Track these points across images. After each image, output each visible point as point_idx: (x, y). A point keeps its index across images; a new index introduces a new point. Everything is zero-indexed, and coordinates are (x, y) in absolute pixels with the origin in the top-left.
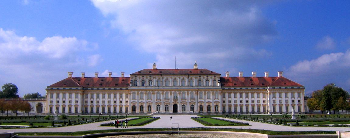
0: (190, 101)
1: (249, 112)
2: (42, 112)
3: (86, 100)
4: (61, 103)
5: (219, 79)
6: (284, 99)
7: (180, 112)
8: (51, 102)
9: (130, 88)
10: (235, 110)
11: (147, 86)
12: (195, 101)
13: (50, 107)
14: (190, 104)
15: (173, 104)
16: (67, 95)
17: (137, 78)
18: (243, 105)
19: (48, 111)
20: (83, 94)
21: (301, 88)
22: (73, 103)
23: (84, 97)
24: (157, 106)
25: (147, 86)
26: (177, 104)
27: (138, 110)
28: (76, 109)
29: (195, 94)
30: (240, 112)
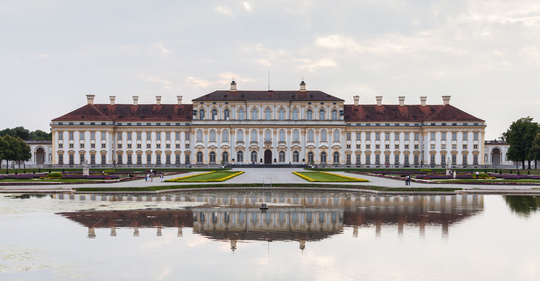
0: (292, 146)
1: (390, 164)
2: (45, 163)
3: (120, 142)
4: (77, 148)
5: (342, 109)
6: (449, 143)
8: (61, 146)
10: (367, 161)
11: (221, 120)
12: (300, 146)
13: (60, 155)
14: (292, 150)
15: (264, 150)
16: (87, 134)
17: (205, 106)
18: (380, 152)
19: (56, 161)
20: (114, 133)
21: (480, 124)
22: (98, 148)
23: (116, 139)
25: (221, 120)
26: (271, 150)
27: (206, 159)
28: (104, 158)
29: (300, 134)
30: (376, 164)
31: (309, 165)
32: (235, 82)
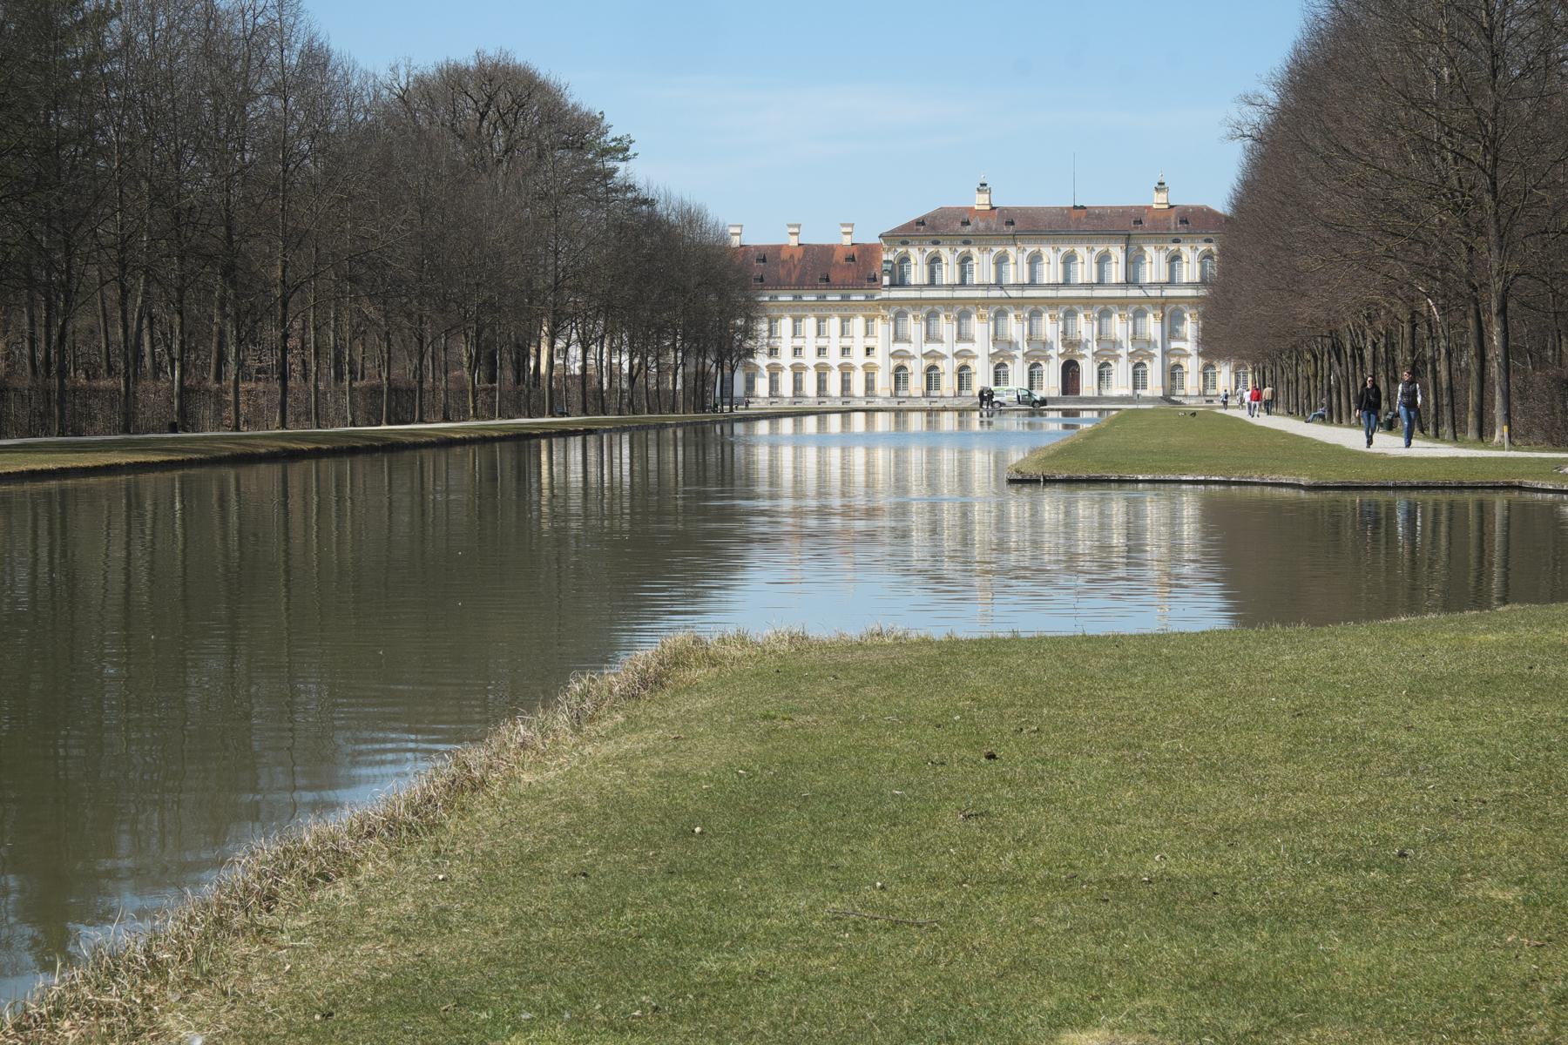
0: (1131, 350)
7: (1090, 395)
9: (885, 294)
15: (1062, 361)
24: (998, 366)
26: (1080, 362)
27: (916, 384)
31: (1173, 398)
32: (988, 186)
